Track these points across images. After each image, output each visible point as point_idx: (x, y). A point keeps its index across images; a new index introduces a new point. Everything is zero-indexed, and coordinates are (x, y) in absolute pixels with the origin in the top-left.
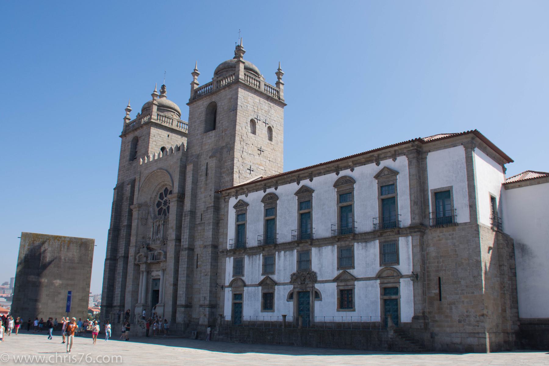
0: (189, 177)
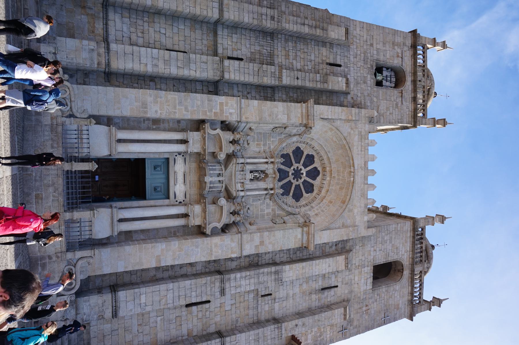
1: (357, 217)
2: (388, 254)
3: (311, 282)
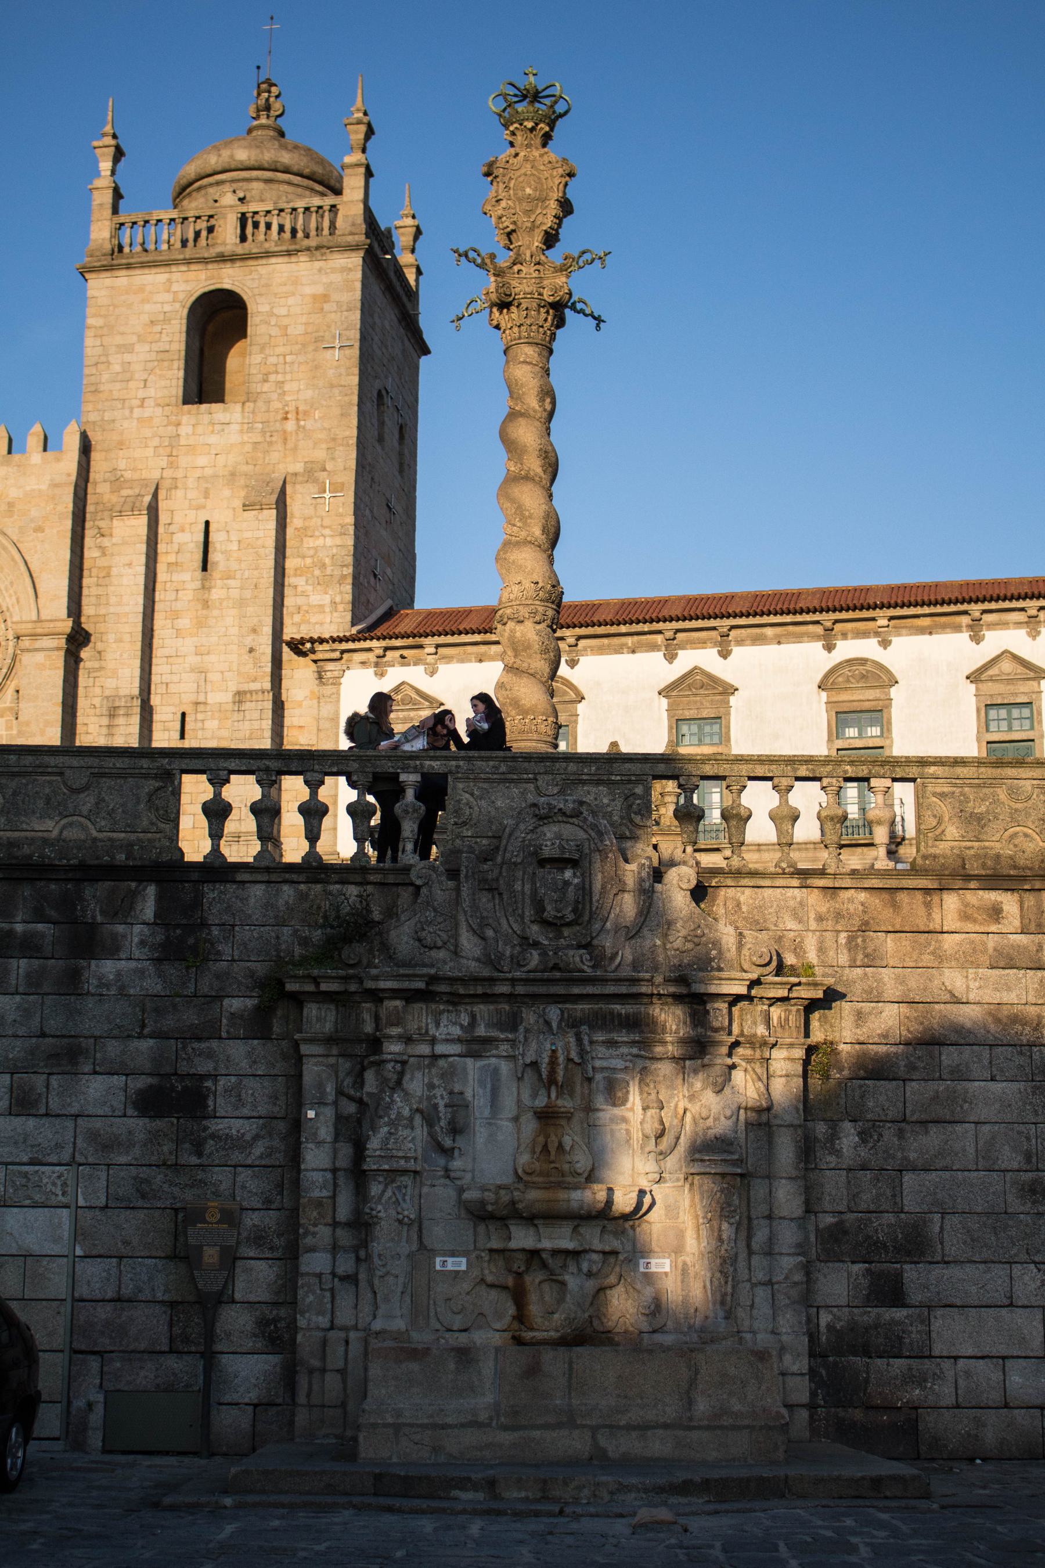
0: (130, 565)
1: (28, 488)
2: (161, 356)
3: (179, 606)
